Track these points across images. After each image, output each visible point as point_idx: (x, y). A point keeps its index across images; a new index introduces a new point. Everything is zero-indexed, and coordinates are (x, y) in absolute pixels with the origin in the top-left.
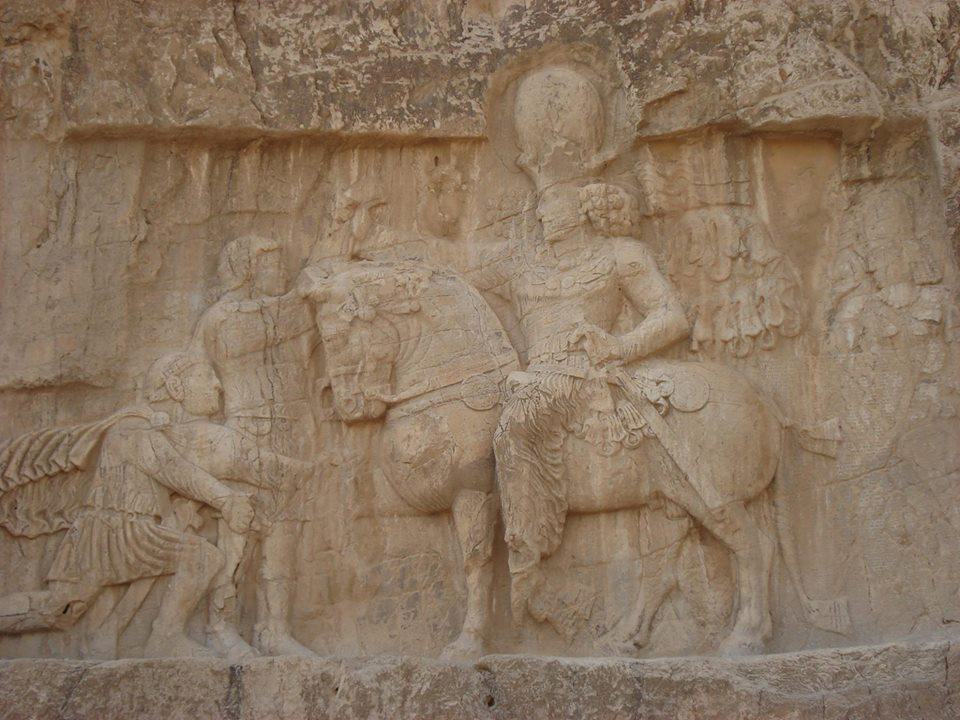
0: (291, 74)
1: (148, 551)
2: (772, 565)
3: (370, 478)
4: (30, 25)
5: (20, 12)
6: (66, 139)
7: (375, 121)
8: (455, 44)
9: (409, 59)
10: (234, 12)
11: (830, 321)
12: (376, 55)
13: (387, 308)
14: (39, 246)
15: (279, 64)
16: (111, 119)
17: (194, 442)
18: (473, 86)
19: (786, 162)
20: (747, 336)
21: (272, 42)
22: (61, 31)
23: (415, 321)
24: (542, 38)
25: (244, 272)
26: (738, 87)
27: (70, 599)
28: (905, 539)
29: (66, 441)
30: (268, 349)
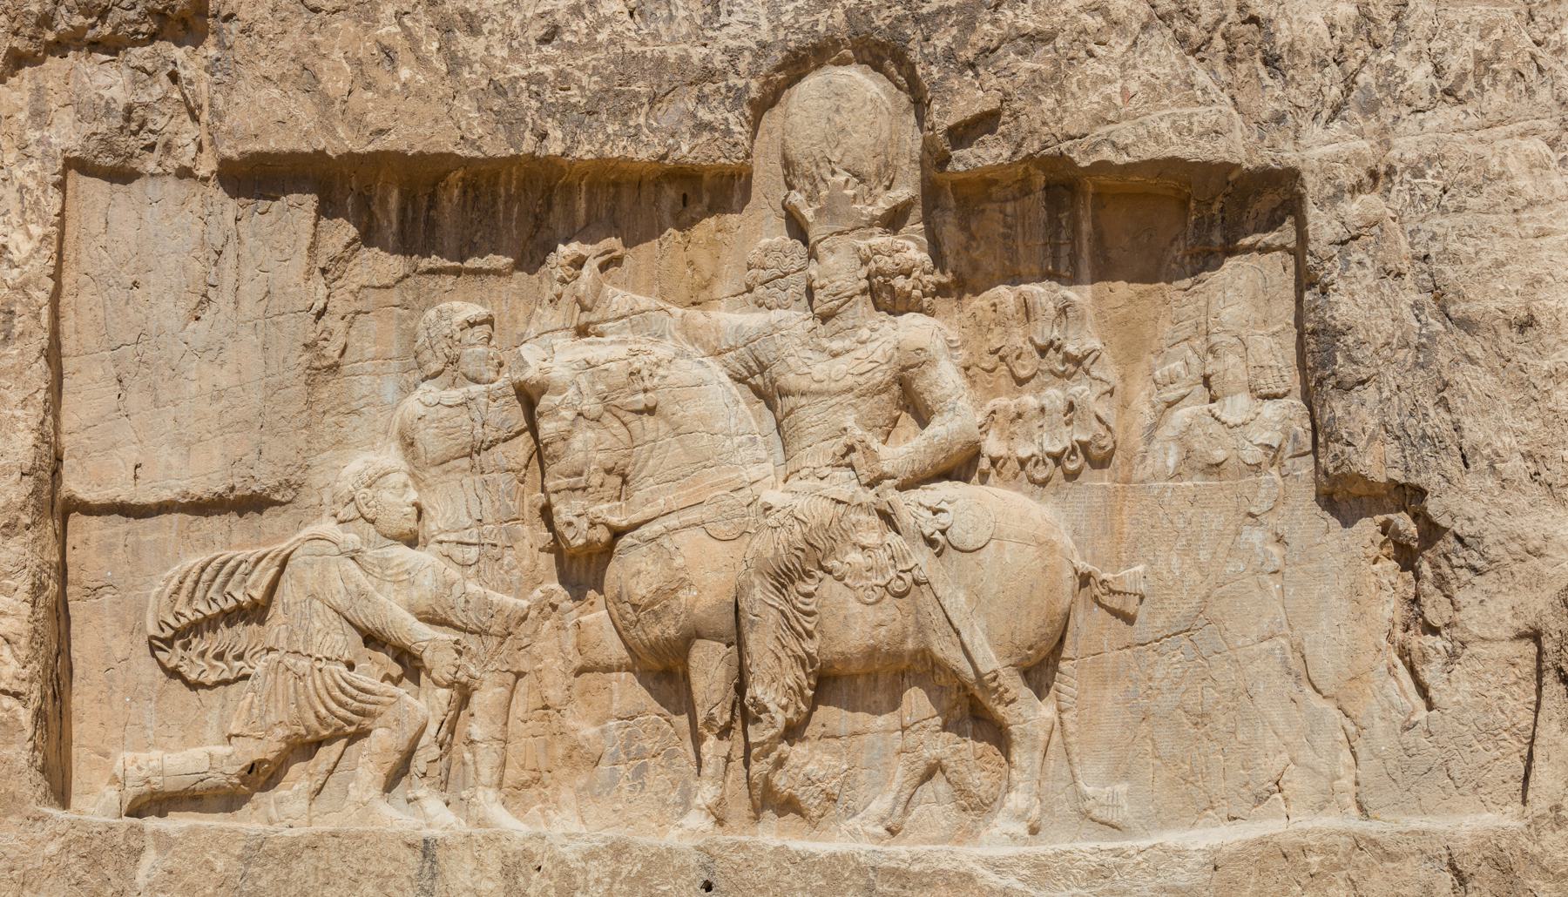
0: (499, 77)
1: (341, 704)
8: (710, 33)
11: (1150, 439)
14: (197, 319)
17: (389, 572)
18: (731, 95)
24: (821, 28)
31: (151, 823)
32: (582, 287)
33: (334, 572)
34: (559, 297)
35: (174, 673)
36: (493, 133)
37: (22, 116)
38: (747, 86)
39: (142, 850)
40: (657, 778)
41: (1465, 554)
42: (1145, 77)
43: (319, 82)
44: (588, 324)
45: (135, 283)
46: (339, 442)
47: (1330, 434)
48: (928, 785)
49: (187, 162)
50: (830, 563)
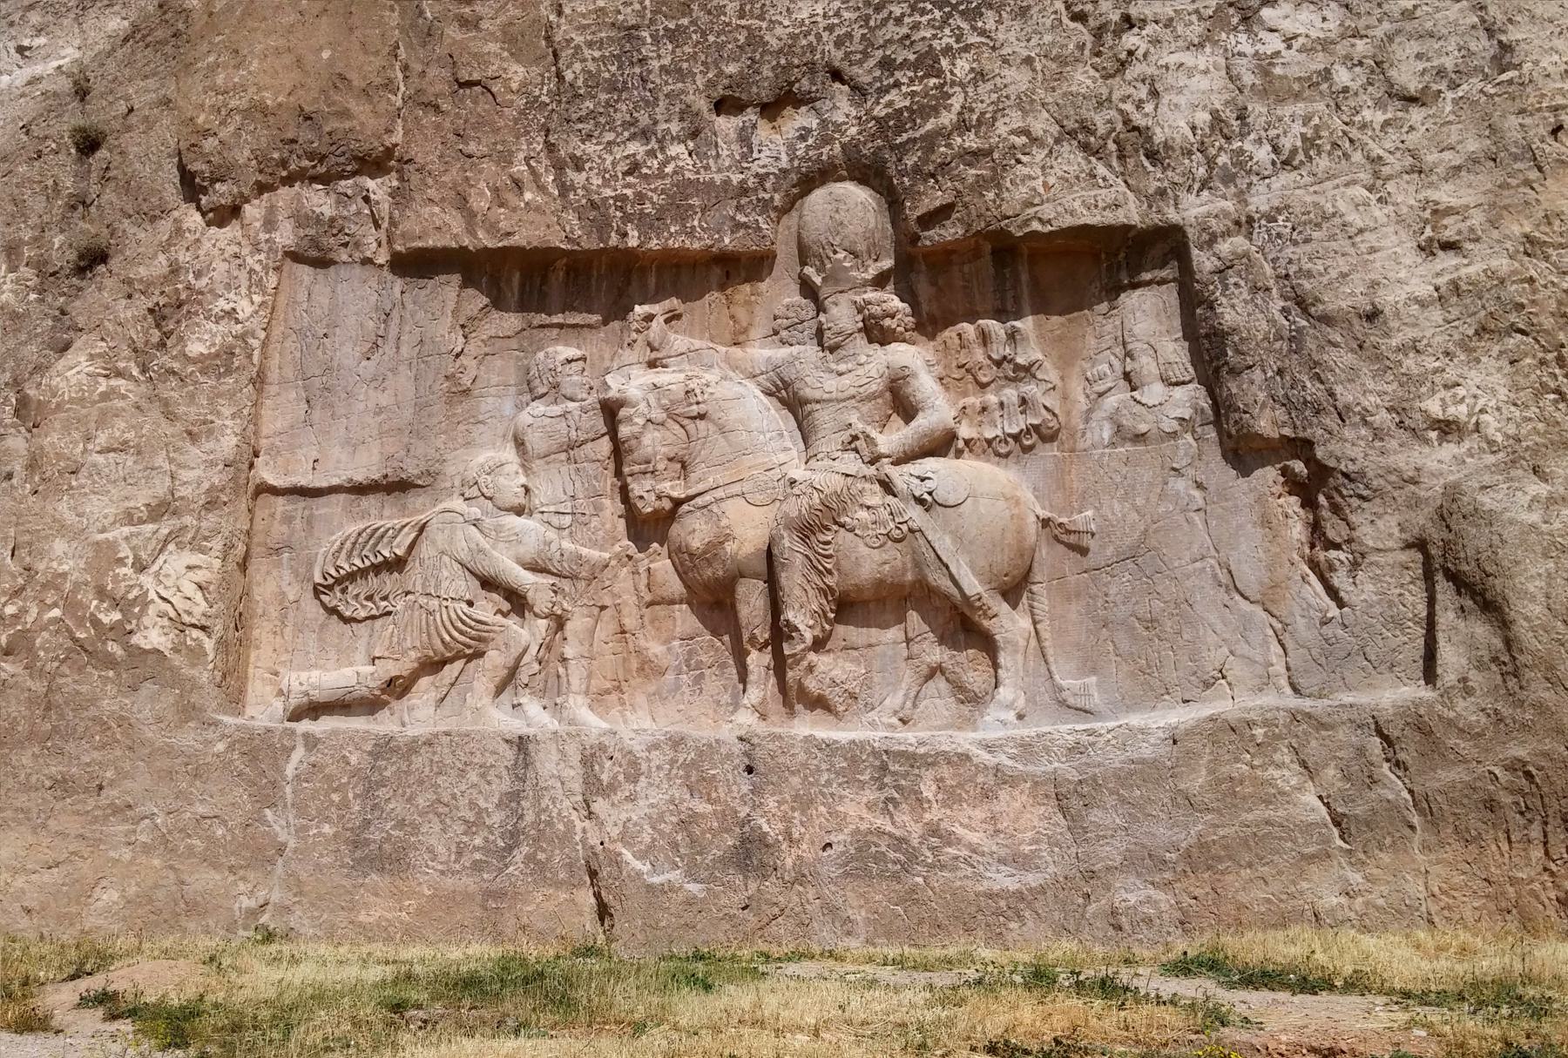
1: (461, 632)
7: (667, 240)
8: (745, 165)
10: (545, 142)
11: (1087, 421)
15: (584, 187)
16: (431, 242)
21: (579, 168)
24: (824, 158)
26: (1003, 200)
31: (305, 726)
32: (652, 335)
33: (460, 534)
34: (635, 341)
35: (333, 611)
36: (589, 235)
37: (258, 224)
39: (294, 748)
40: (712, 684)
41: (1353, 486)
42: (1060, 173)
44: (656, 360)
46: (469, 443)
47: (1230, 406)
48: (930, 682)
49: (368, 254)
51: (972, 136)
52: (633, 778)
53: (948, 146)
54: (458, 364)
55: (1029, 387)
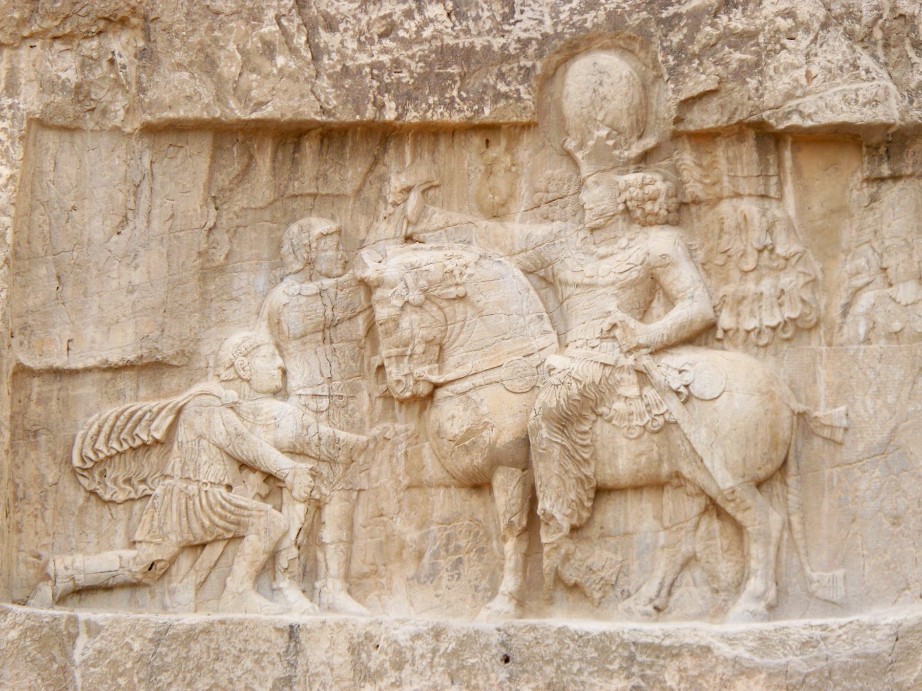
0: (349, 63)
1: (222, 517)
2: (781, 538)
3: (419, 453)
4: (105, 19)
5: (96, 7)
6: (141, 130)
7: (426, 111)
8: (506, 27)
9: (461, 46)
11: (845, 314)
12: (430, 42)
13: (435, 293)
14: (119, 233)
17: (260, 418)
18: (522, 72)
19: (812, 162)
20: (767, 327)
22: (134, 21)
23: (461, 306)
24: (589, 25)
25: (305, 256)
26: (765, 89)
27: (155, 559)
28: (896, 520)
29: (148, 416)
30: (328, 327)
33: (217, 419)
38: (534, 66)
43: (218, 67)
45: (74, 208)
49: (117, 122)
50: (602, 409)
51: (739, 15)
52: (399, 666)
53: (713, 25)
54: (212, 237)
55: (788, 280)
